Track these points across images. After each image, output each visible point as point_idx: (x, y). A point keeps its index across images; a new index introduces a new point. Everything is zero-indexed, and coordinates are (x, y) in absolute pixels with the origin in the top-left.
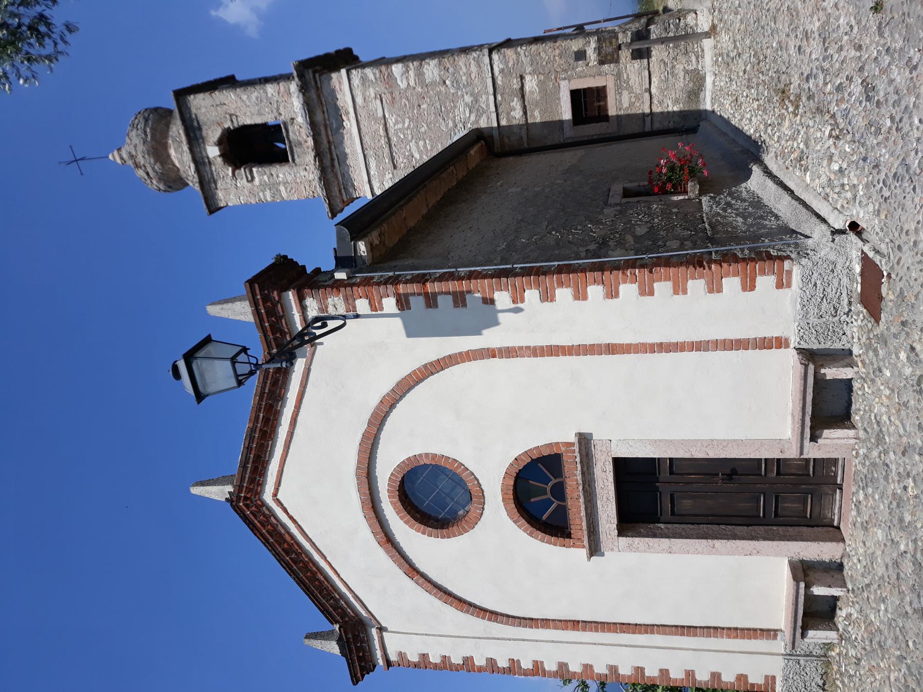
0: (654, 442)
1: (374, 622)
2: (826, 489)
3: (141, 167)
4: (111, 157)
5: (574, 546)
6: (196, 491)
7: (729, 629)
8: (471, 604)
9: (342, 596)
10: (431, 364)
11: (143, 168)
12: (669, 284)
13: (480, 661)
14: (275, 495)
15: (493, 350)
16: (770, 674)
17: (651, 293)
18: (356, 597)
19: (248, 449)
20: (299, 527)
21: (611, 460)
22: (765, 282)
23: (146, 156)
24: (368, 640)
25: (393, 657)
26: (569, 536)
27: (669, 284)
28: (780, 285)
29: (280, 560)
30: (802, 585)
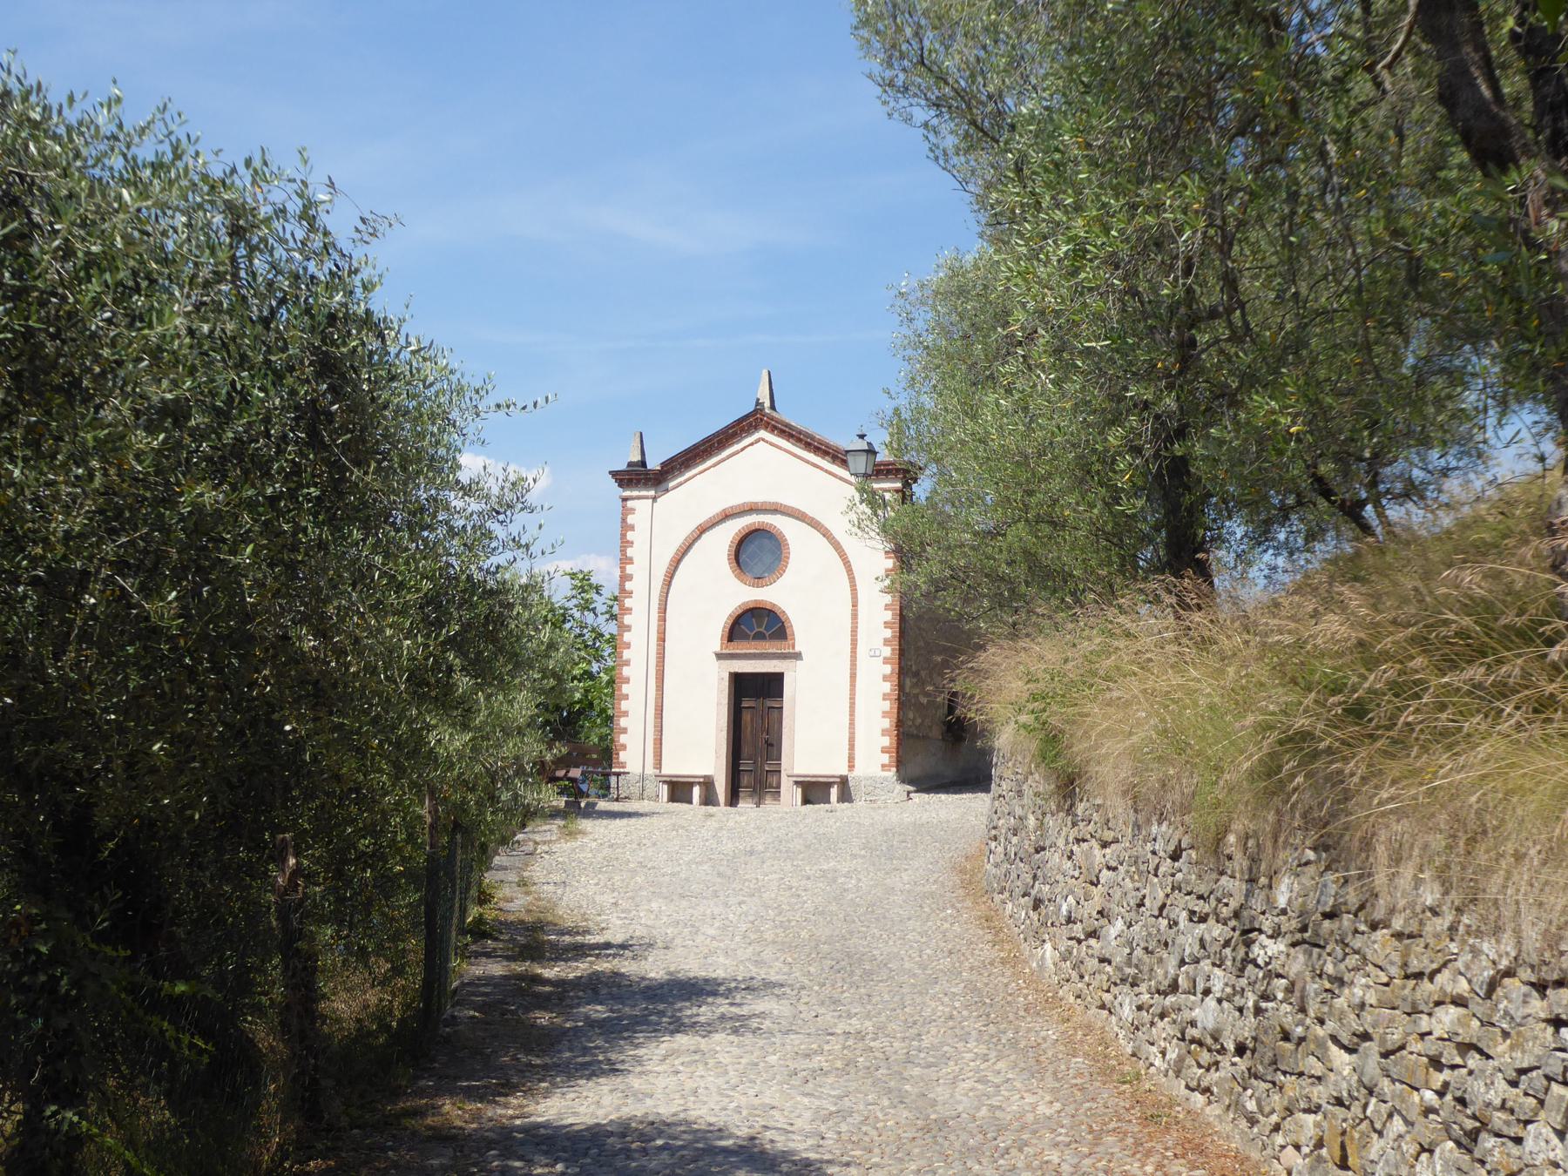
2: (756, 799)
8: (676, 568)
9: (681, 474)
13: (629, 569)
18: (680, 484)
19: (800, 432)
20: (737, 453)
22: (886, 759)
25: (630, 504)
28: (883, 766)
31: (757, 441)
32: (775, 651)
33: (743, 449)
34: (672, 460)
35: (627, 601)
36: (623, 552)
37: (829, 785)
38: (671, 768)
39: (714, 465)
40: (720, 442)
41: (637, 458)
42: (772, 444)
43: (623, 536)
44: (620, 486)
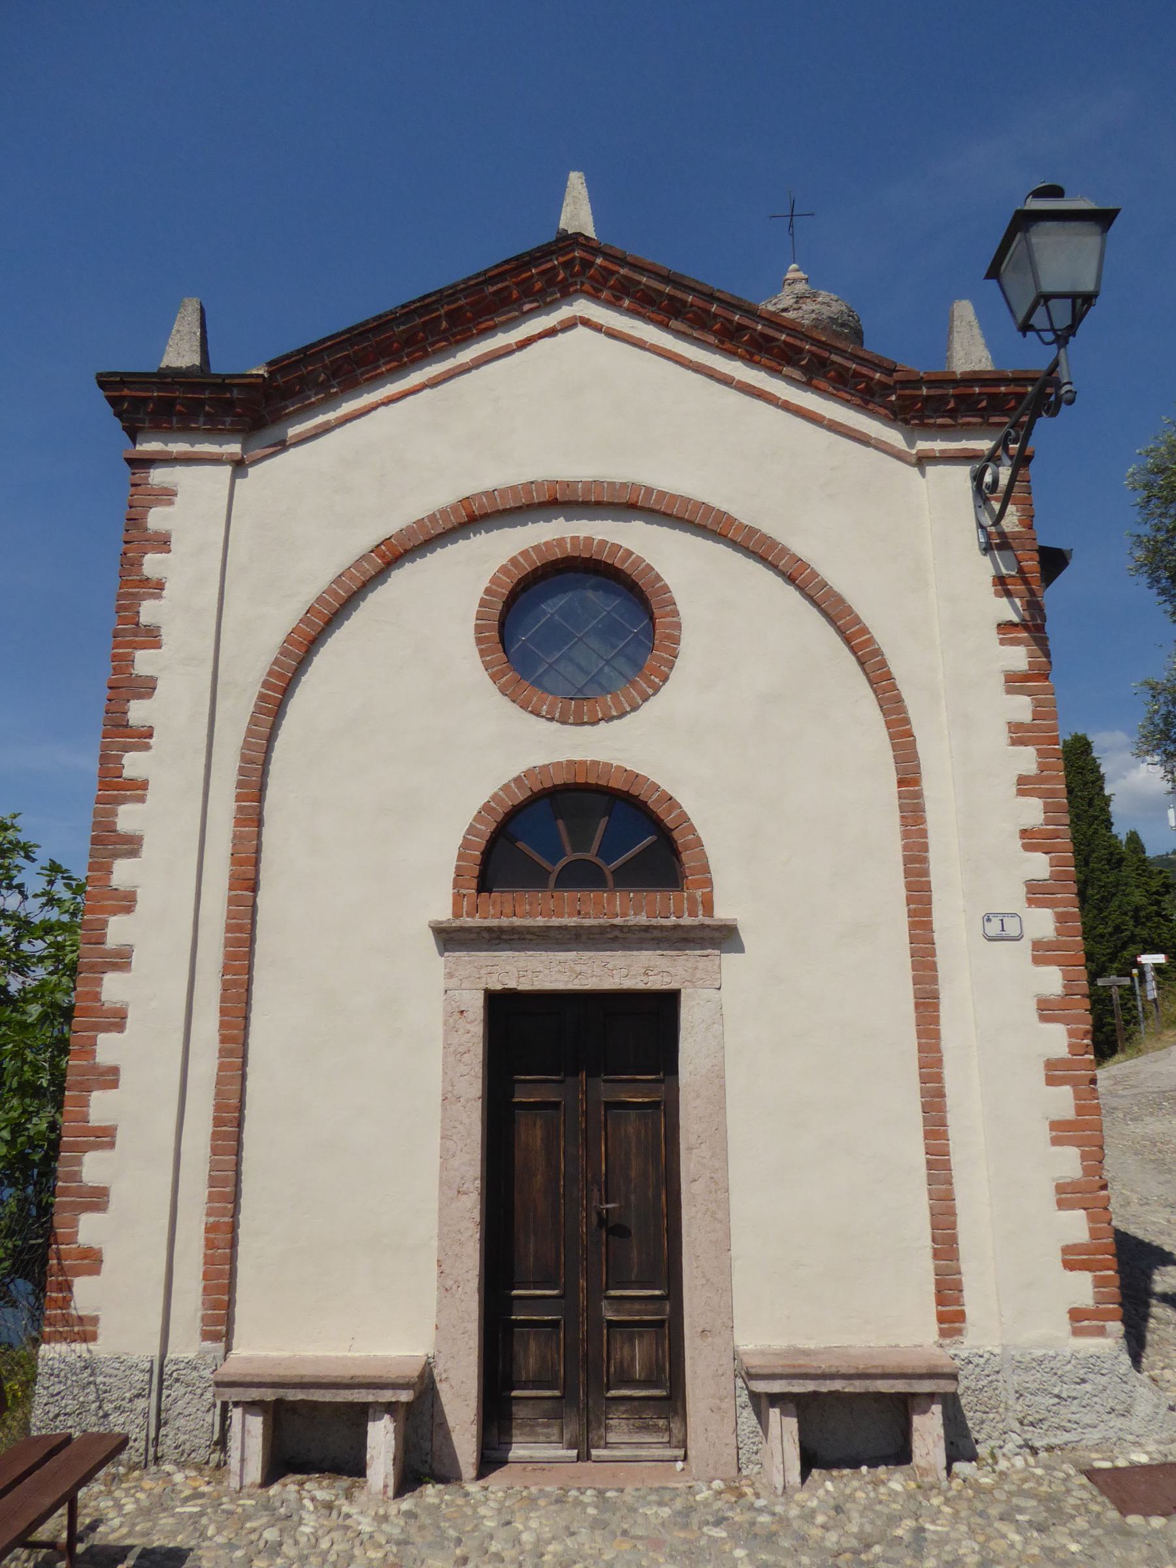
0: (718, 1077)
3: (797, 302)
4: (794, 266)
5: (458, 898)
7: (234, 1227)
9: (330, 401)
10: (883, 664)
11: (795, 306)
14: (586, 322)
15: (916, 782)
16: (102, 1329)
17: (1051, 1081)
18: (326, 429)
20: (506, 352)
21: (674, 986)
23: (814, 316)
24: (215, 431)
25: (158, 476)
26: (484, 884)
28: (1076, 1315)
29: (442, 296)
34: (307, 354)
35: (129, 758)
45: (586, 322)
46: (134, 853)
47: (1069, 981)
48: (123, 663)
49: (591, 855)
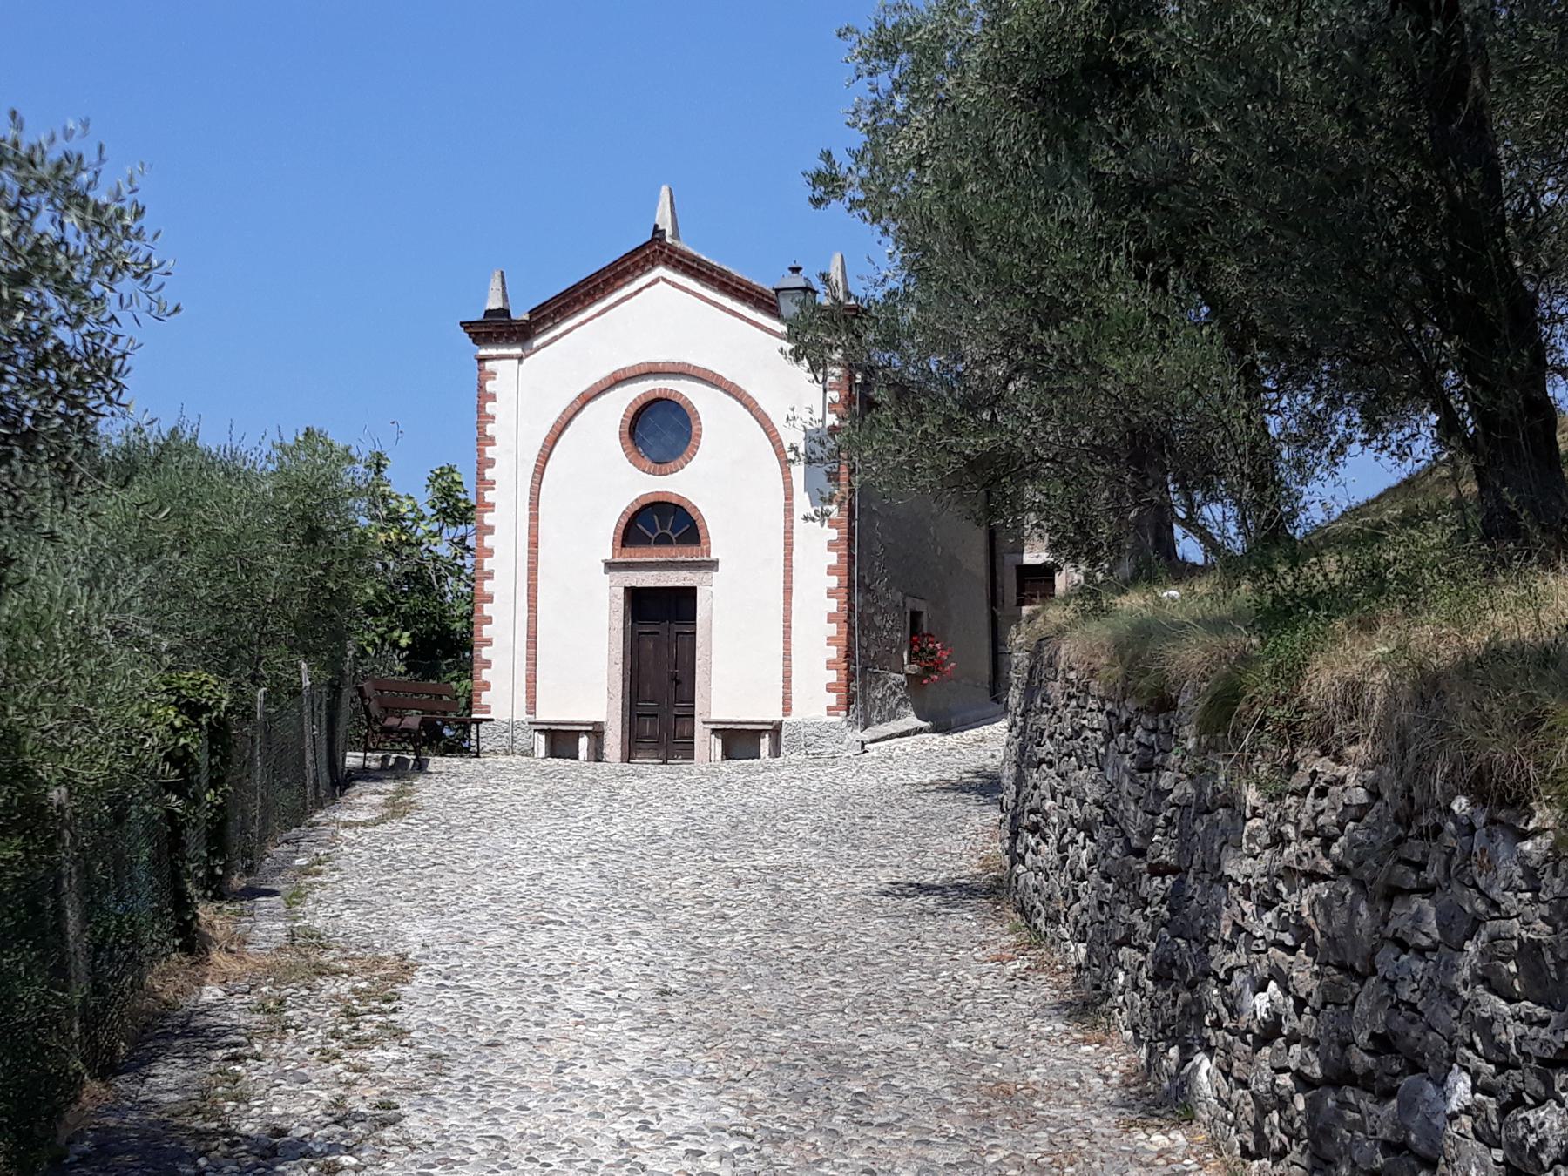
1: (528, 352)
5: (614, 549)
6: (665, 192)
9: (555, 325)
12: (835, 634)
13: (490, 452)
14: (664, 280)
15: (791, 499)
17: (829, 621)
18: (555, 339)
22: (832, 699)
25: (489, 365)
27: (835, 634)
28: (829, 708)
30: (590, 728)
31: (656, 281)
32: (683, 558)
33: (636, 293)
35: (487, 494)
36: (481, 429)
37: (758, 734)
38: (545, 713)
39: (599, 314)
40: (606, 282)
41: (494, 303)
42: (675, 285)
43: (481, 408)
44: (474, 342)
45: (664, 280)
46: (492, 533)
47: (840, 582)
48: (481, 452)
49: (668, 532)
